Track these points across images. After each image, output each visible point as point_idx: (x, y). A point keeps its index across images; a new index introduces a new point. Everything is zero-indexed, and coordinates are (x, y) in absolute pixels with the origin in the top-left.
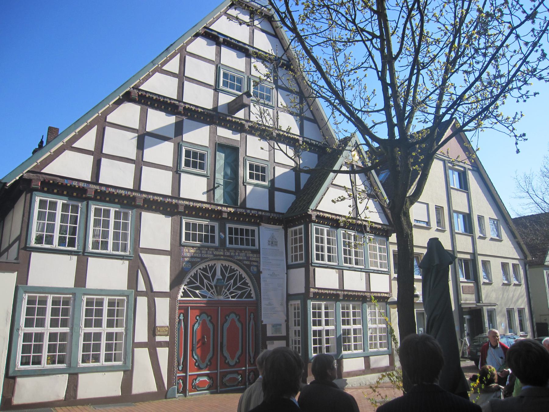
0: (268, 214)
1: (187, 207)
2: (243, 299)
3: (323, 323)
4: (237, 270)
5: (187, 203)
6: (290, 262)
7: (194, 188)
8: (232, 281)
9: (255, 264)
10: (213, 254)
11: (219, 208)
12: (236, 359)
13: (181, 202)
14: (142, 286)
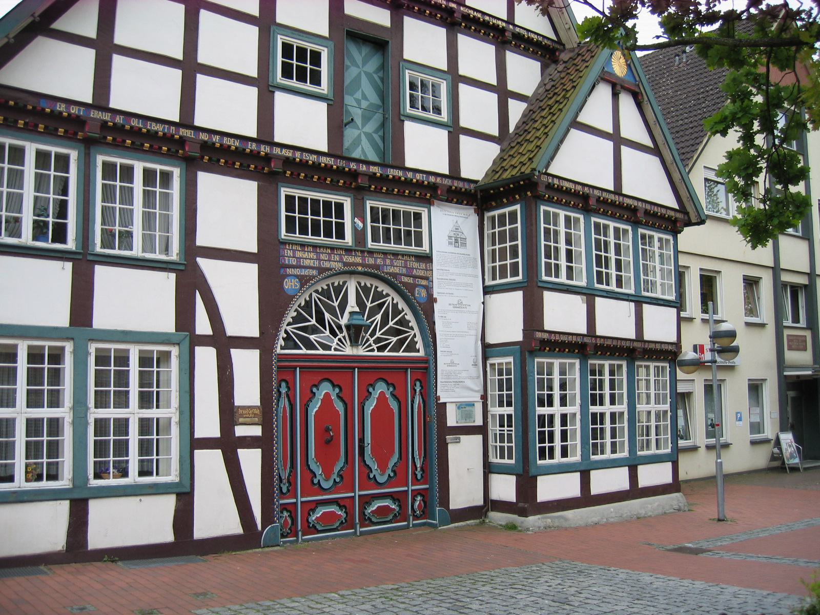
0: (447, 182)
1: (288, 162)
2: (401, 354)
3: (607, 399)
4: (388, 295)
6: (489, 282)
7: (302, 123)
8: (379, 317)
10: (341, 261)
11: (353, 166)
12: (389, 472)
13: (277, 151)
14: (203, 326)
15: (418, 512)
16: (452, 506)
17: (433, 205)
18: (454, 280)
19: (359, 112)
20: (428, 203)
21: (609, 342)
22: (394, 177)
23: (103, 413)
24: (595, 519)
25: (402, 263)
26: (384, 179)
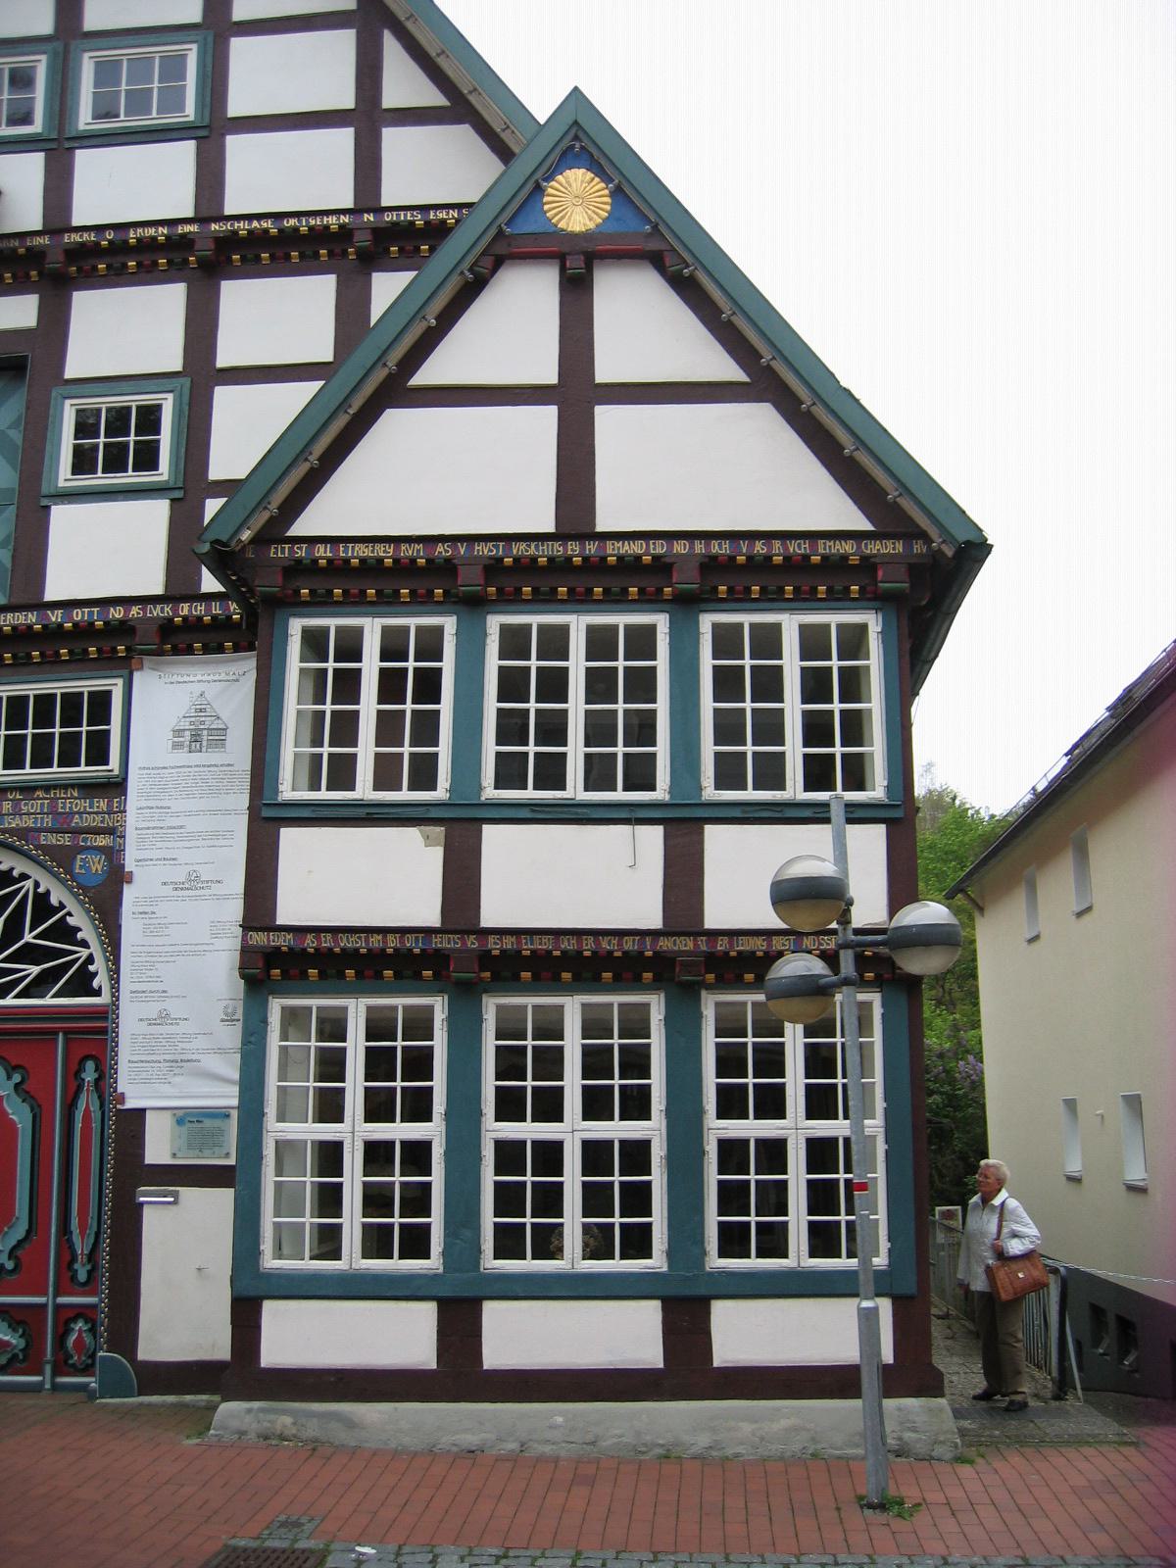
2: (48, 1001)
4: (24, 877)
9: (102, 841)
15: (76, 1358)
16: (146, 1352)
17: (141, 668)
18: (181, 827)
20: (125, 666)
21: (544, 944)
22: (15, 628)
23: (415, 1131)
24: (471, 1439)
25: (42, 805)
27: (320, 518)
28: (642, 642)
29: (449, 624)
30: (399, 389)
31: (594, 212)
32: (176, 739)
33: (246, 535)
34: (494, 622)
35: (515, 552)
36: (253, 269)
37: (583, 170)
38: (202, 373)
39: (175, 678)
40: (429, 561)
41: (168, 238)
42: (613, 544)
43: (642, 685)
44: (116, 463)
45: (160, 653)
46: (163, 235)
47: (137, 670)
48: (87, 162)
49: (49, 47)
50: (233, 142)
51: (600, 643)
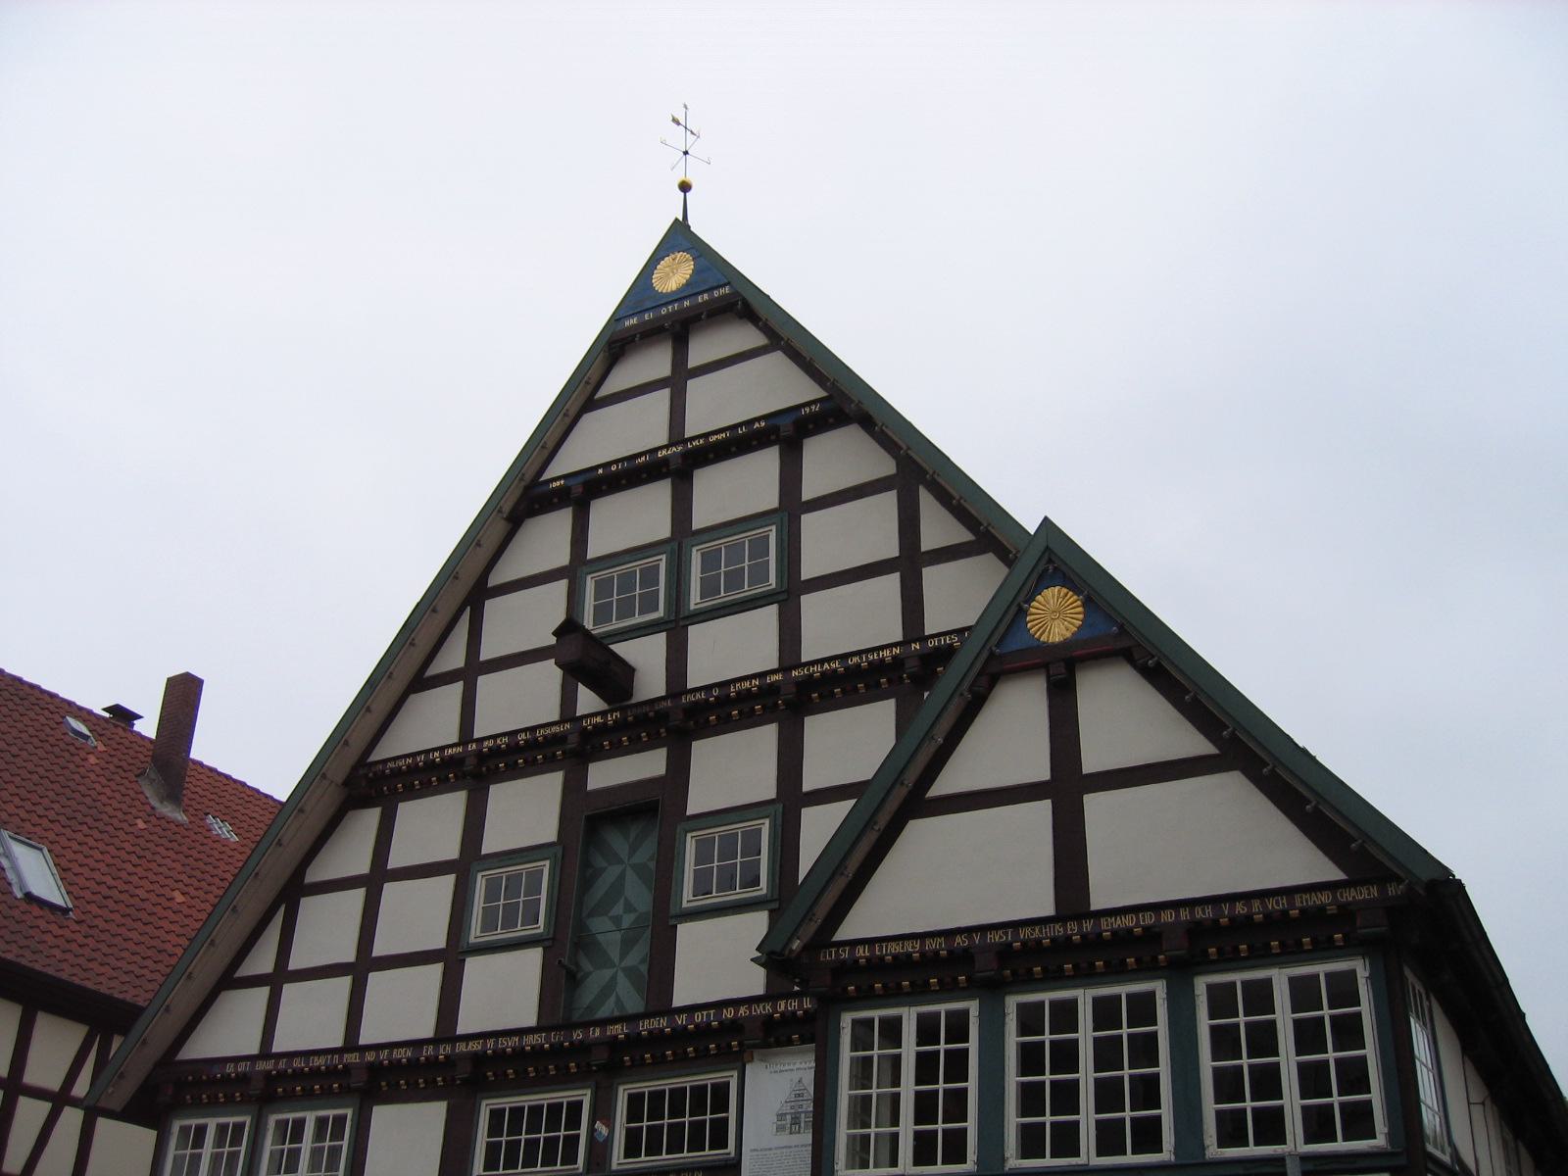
1: (478, 1059)
5: (475, 1046)
7: (505, 993)
11: (578, 1035)
13: (461, 1047)
17: (751, 1060)
19: (618, 936)
20: (738, 1060)
22: (650, 1032)
26: (634, 1041)
27: (858, 924)
28: (1142, 1009)
29: (973, 1007)
30: (918, 803)
31: (1069, 622)
32: (779, 1123)
33: (796, 945)
34: (1012, 1002)
35: (1022, 937)
36: (830, 704)
37: (1057, 588)
38: (792, 798)
39: (779, 1067)
40: (950, 952)
41: (759, 687)
42: (1107, 920)
43: (1145, 1051)
44: (727, 884)
45: (769, 1046)
46: (756, 686)
47: (749, 1062)
48: (699, 636)
49: (668, 547)
50: (807, 601)
51: (1105, 1014)
